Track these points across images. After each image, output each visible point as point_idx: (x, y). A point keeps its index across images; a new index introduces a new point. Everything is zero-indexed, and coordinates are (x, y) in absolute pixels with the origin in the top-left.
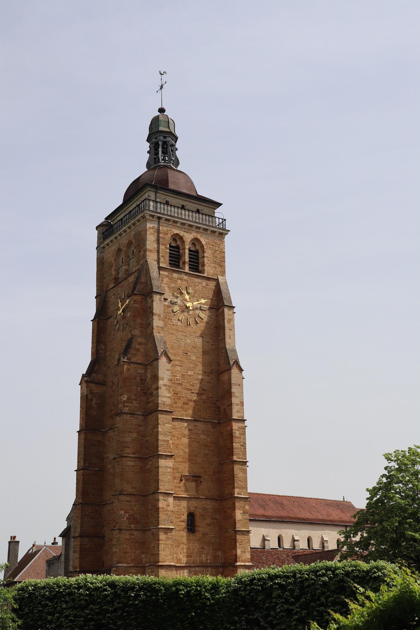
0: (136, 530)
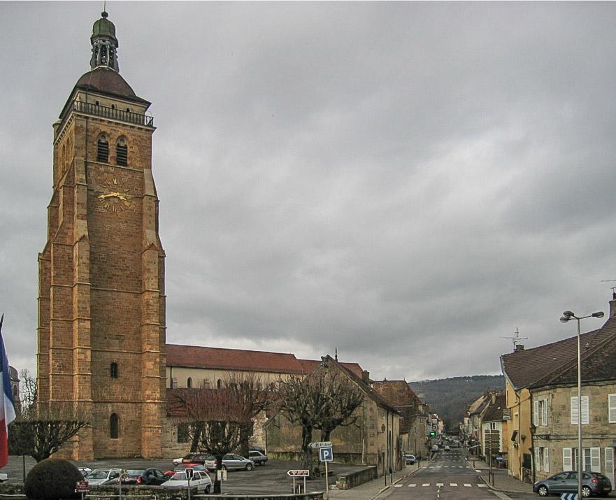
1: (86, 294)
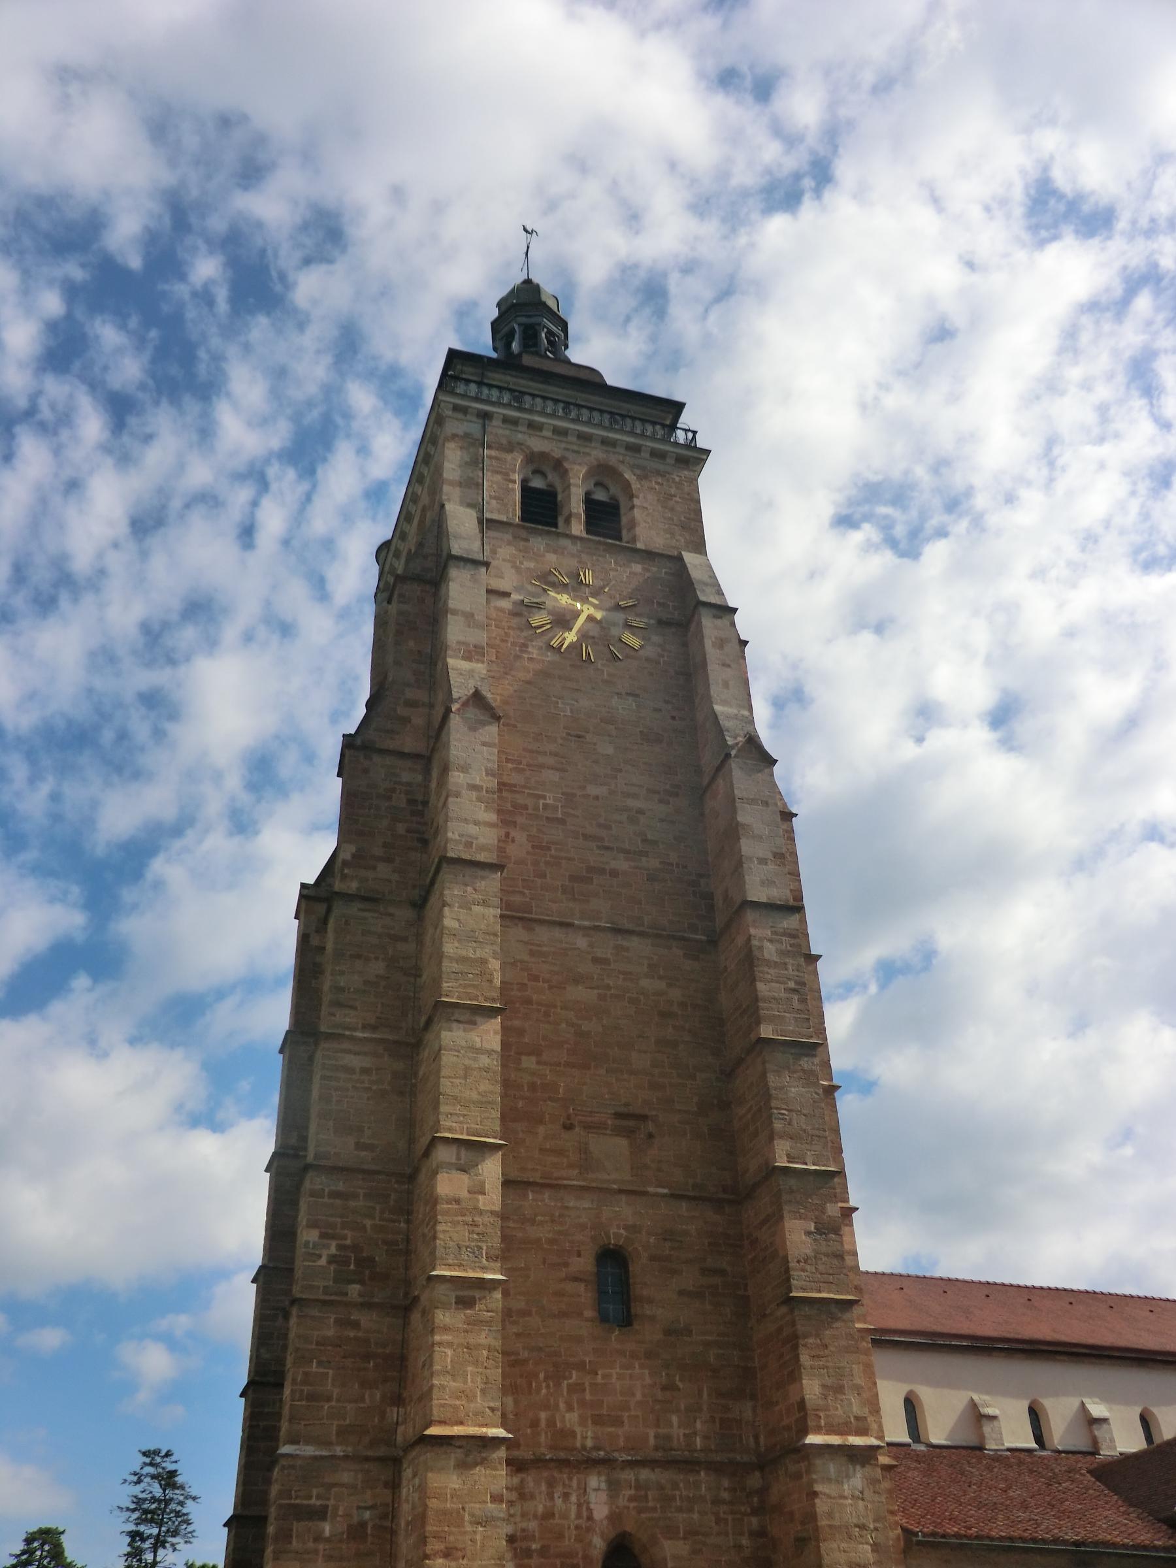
0: (367, 1306)
1: (484, 903)
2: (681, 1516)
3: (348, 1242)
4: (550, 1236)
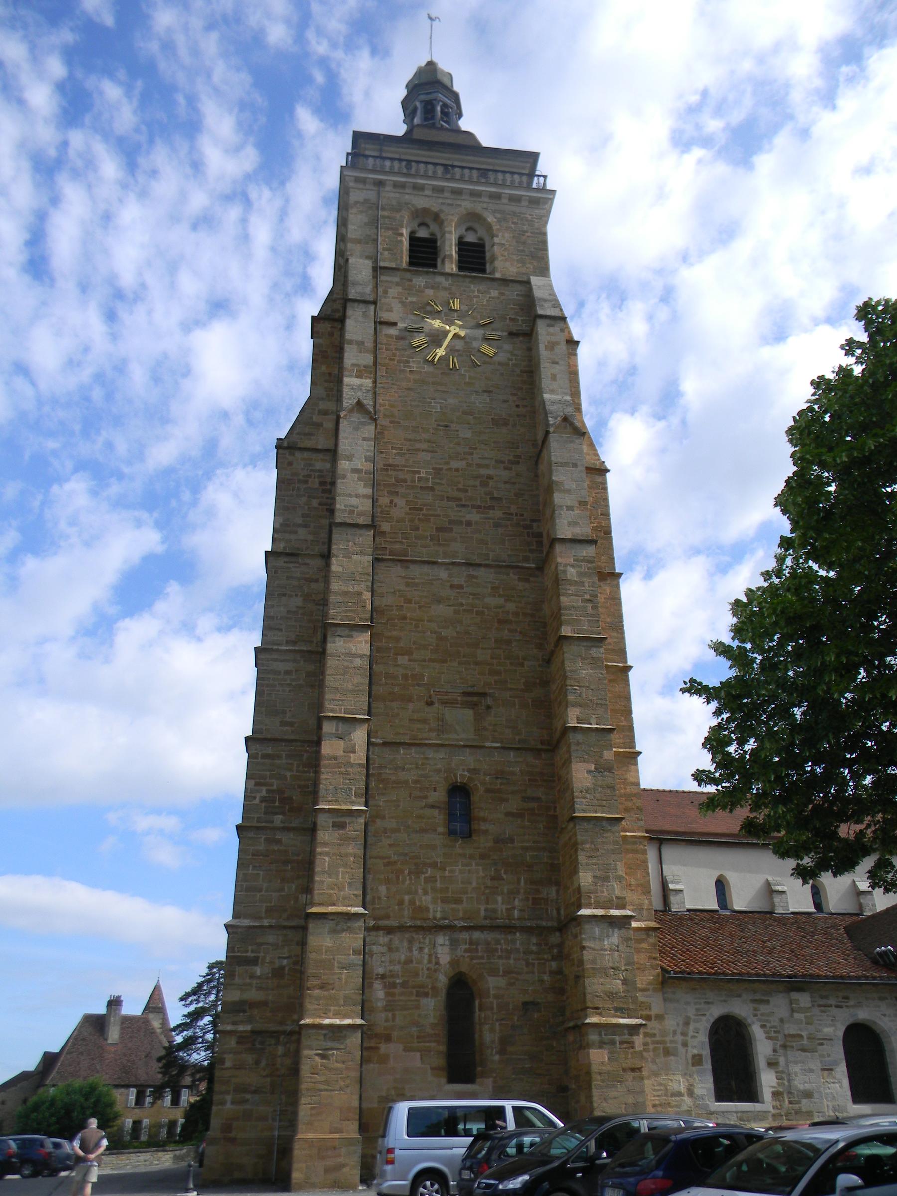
1: (361, 553)
2: (501, 962)
3: (275, 788)
4: (415, 778)
